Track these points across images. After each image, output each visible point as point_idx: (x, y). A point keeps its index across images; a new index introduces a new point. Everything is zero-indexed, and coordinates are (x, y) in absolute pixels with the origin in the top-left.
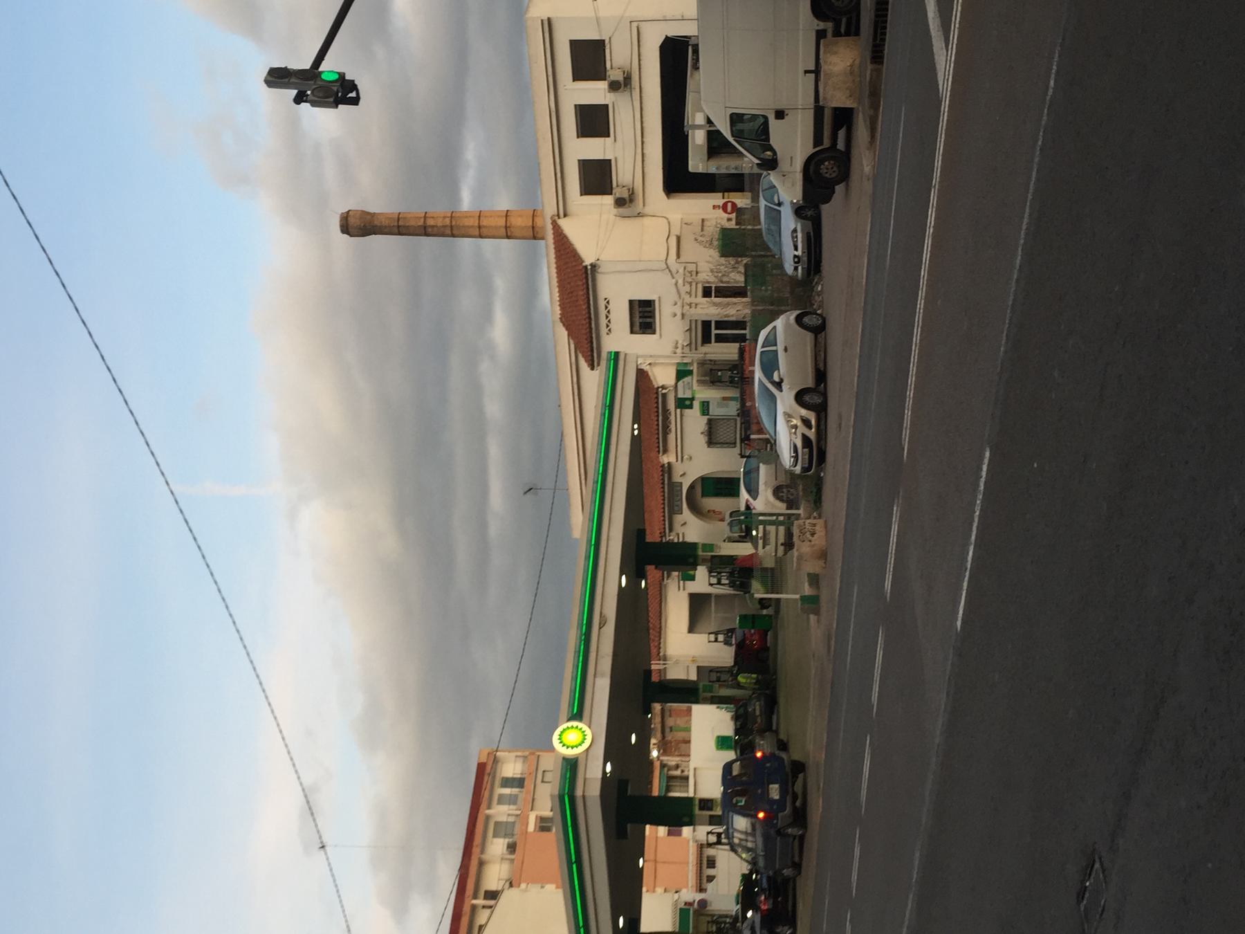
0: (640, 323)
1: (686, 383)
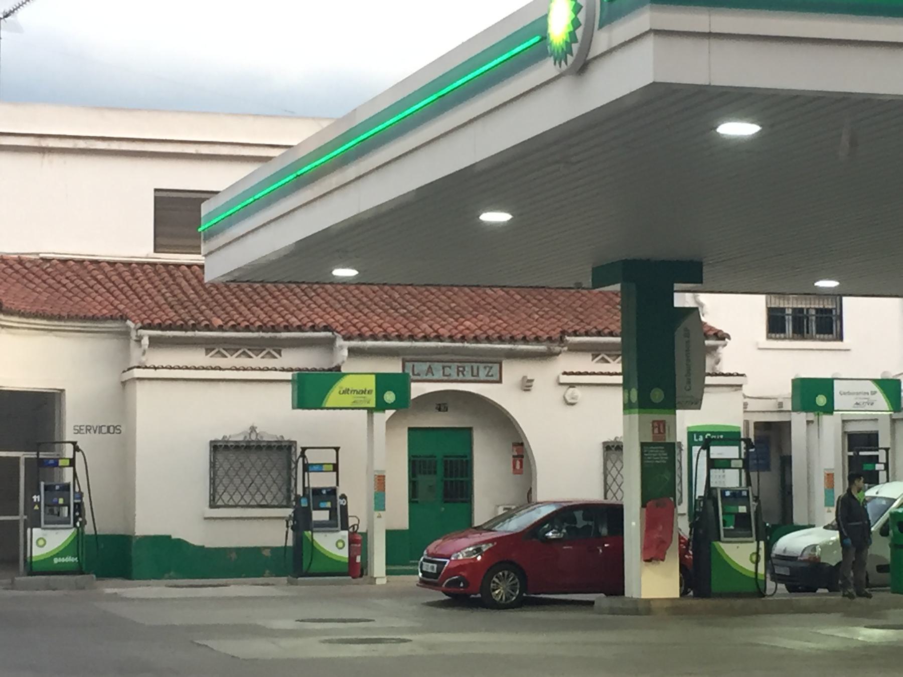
0: (783, 310)
1: (872, 398)
